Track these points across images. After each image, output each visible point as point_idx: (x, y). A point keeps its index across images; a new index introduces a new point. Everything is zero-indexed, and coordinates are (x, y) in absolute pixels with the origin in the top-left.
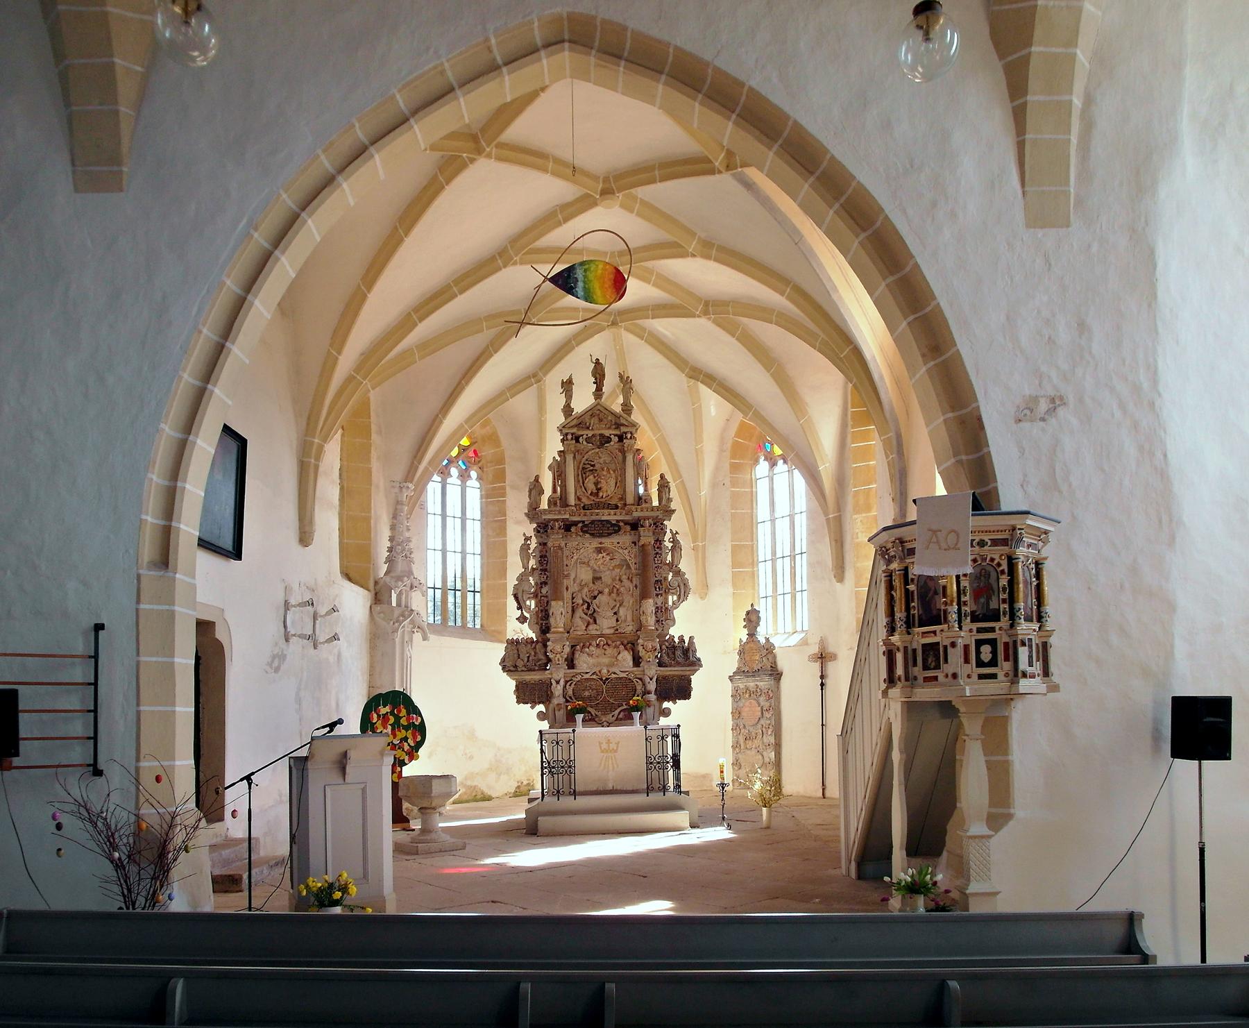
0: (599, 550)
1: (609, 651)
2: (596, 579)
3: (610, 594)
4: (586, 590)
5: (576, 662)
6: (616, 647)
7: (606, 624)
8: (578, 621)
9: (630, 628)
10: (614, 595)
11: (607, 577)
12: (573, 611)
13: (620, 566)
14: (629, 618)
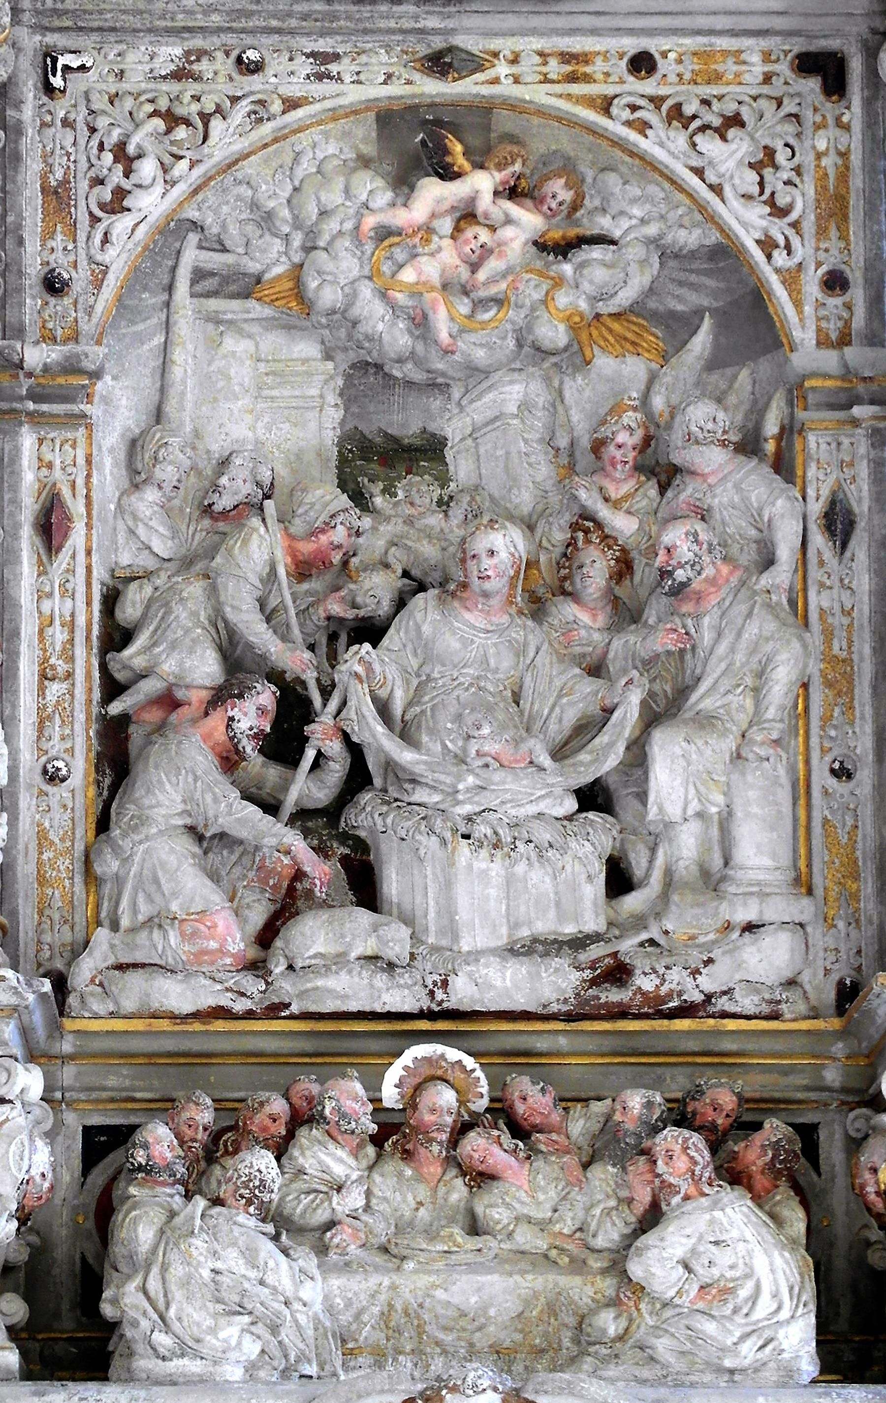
0: (418, 144)
1: (529, 1192)
2: (381, 458)
3: (541, 592)
4: (260, 548)
5: (124, 1299)
6: (613, 1145)
7: (491, 900)
8: (158, 858)
9: (768, 960)
10: (583, 619)
11: (501, 432)
12: (117, 758)
13: (654, 325)
14: (760, 851)
